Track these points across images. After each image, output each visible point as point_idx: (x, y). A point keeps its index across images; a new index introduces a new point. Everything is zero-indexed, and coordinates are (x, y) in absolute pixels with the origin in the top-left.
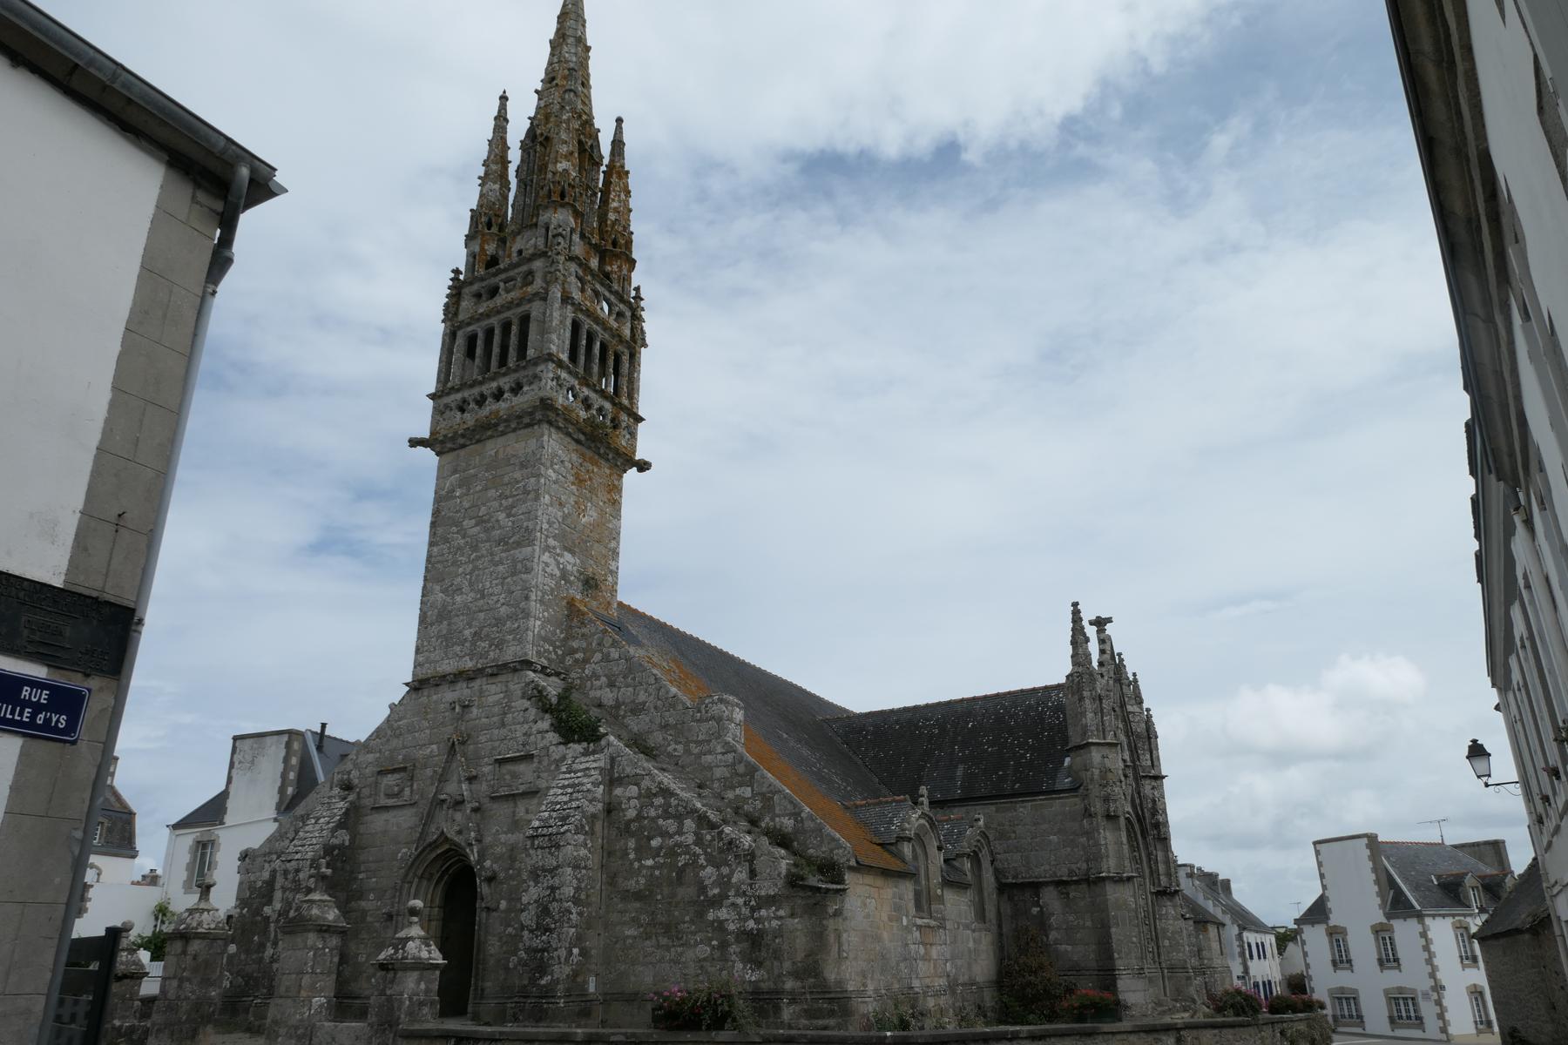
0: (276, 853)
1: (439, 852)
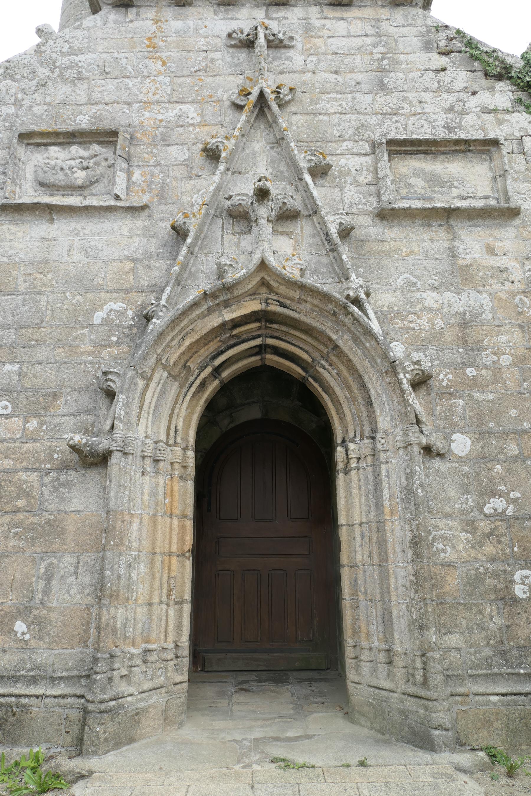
1: (229, 315)
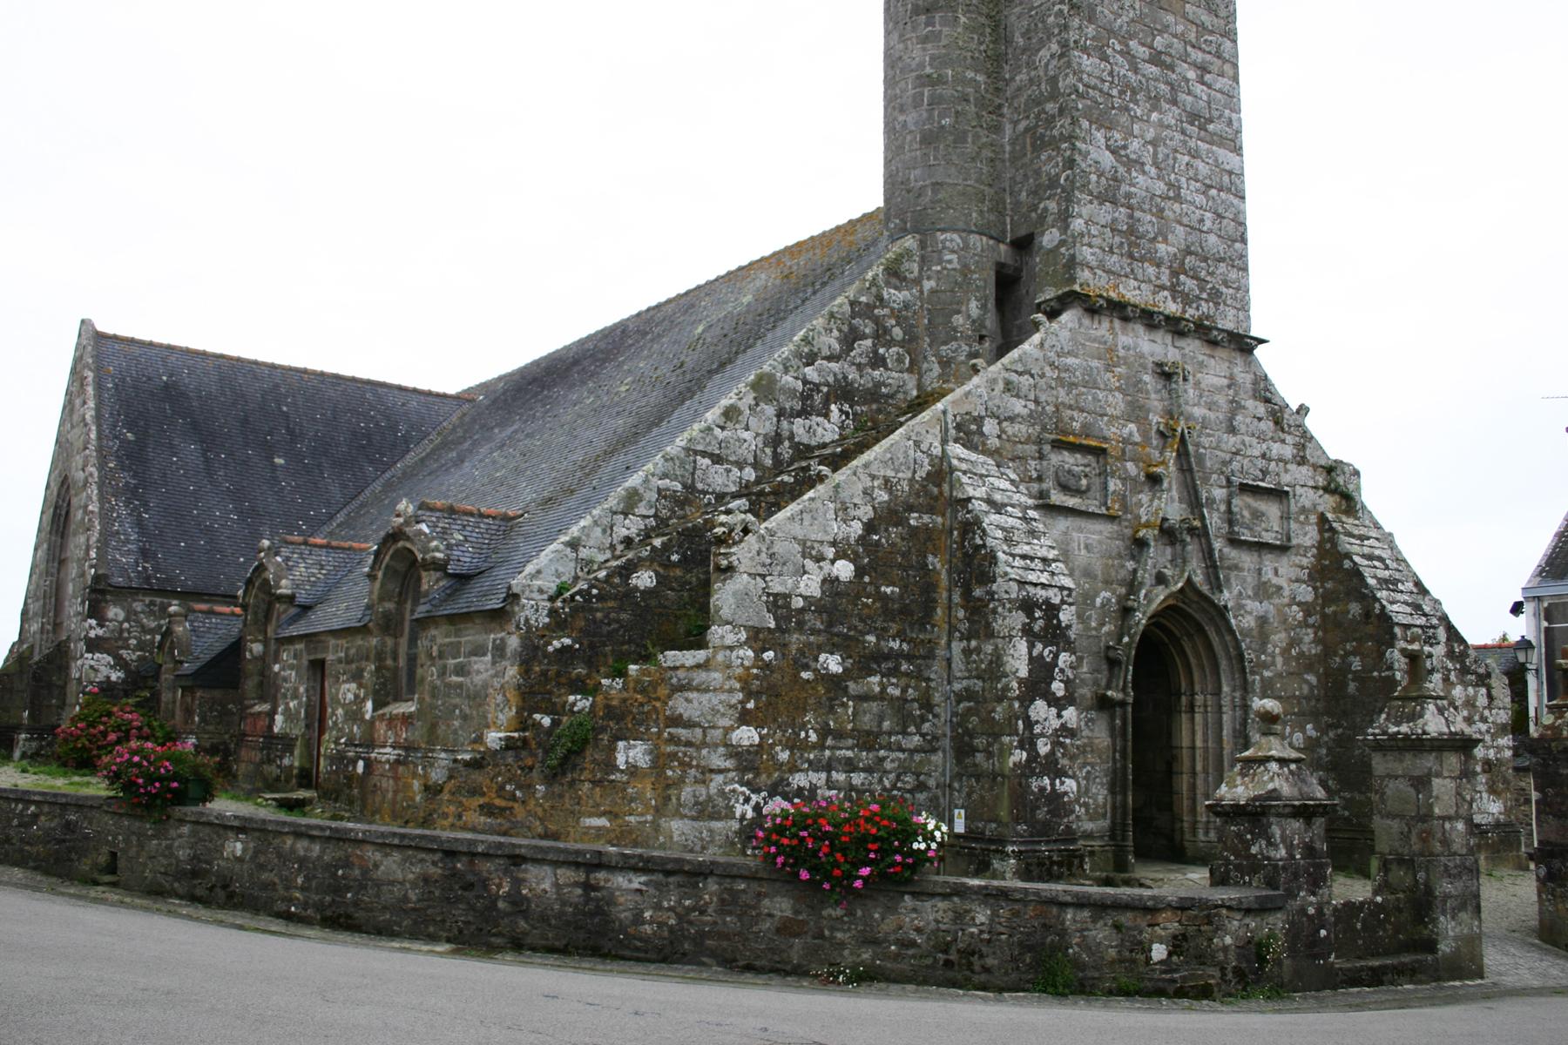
0: (834, 544)
